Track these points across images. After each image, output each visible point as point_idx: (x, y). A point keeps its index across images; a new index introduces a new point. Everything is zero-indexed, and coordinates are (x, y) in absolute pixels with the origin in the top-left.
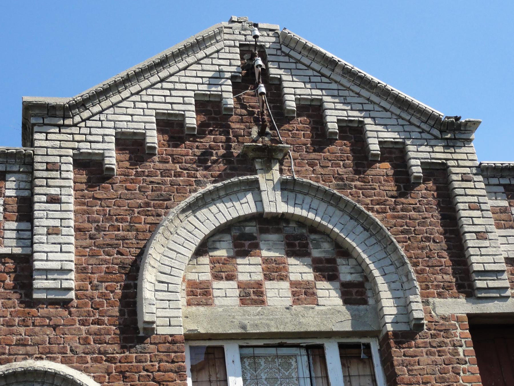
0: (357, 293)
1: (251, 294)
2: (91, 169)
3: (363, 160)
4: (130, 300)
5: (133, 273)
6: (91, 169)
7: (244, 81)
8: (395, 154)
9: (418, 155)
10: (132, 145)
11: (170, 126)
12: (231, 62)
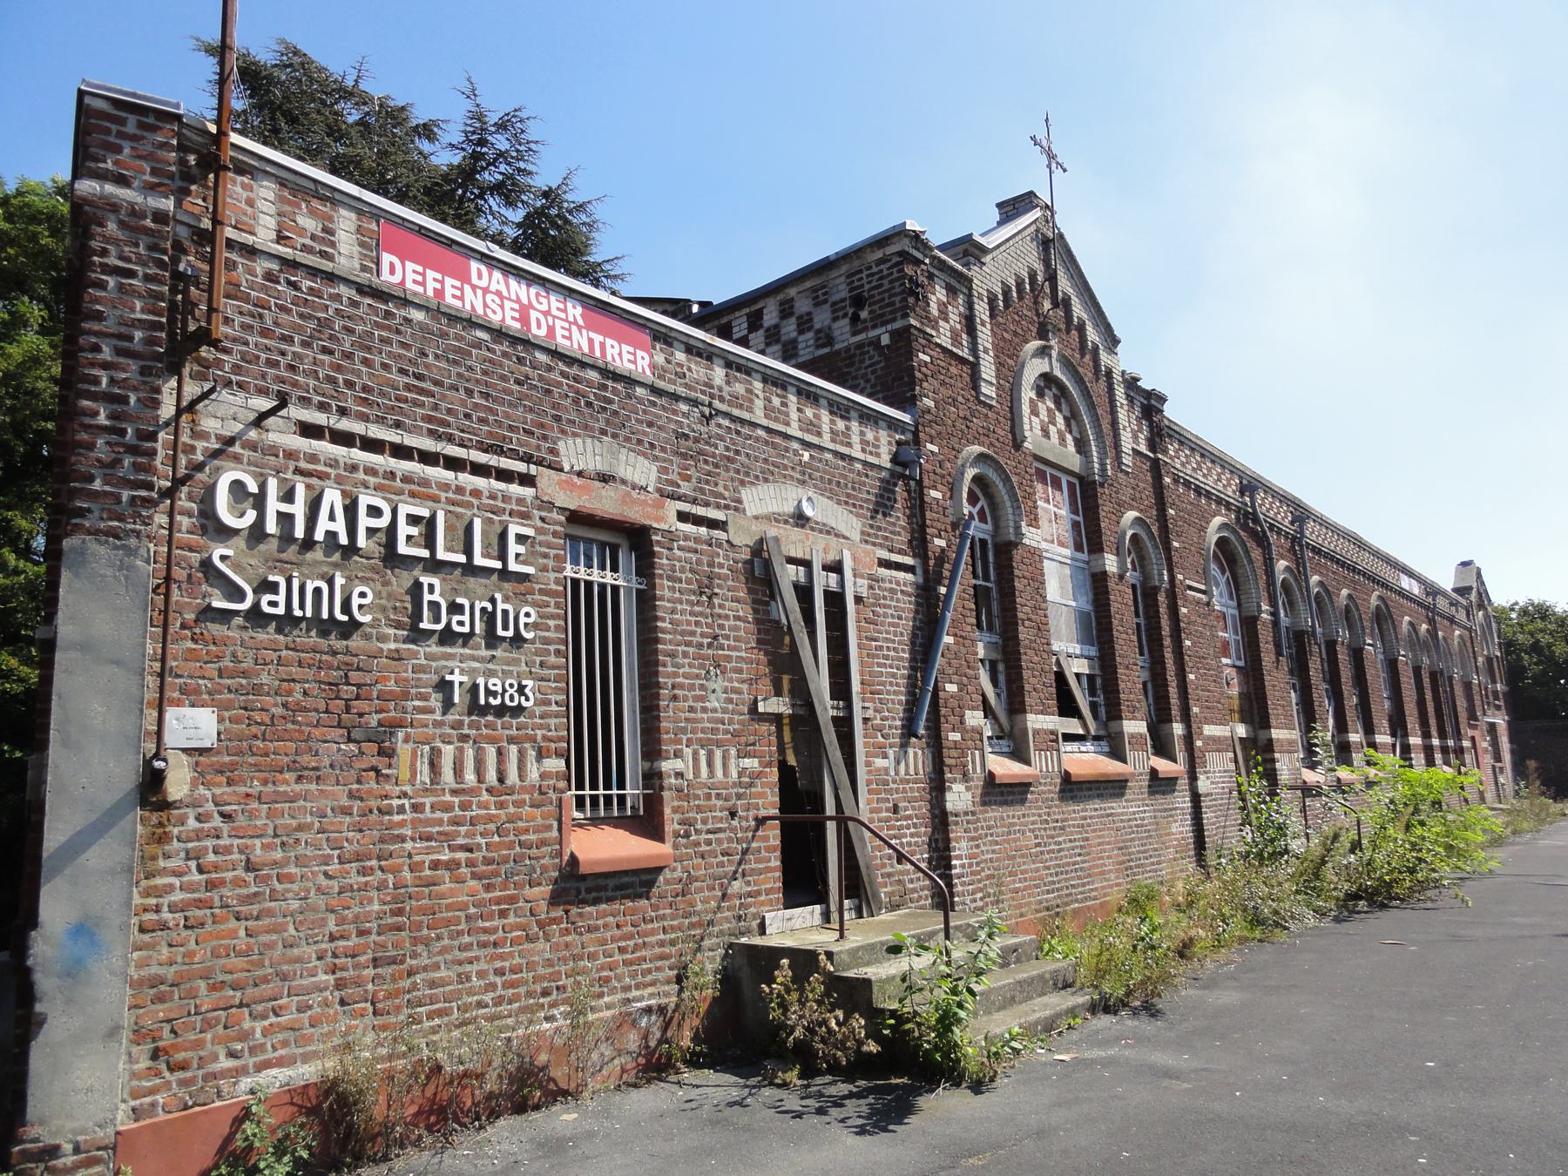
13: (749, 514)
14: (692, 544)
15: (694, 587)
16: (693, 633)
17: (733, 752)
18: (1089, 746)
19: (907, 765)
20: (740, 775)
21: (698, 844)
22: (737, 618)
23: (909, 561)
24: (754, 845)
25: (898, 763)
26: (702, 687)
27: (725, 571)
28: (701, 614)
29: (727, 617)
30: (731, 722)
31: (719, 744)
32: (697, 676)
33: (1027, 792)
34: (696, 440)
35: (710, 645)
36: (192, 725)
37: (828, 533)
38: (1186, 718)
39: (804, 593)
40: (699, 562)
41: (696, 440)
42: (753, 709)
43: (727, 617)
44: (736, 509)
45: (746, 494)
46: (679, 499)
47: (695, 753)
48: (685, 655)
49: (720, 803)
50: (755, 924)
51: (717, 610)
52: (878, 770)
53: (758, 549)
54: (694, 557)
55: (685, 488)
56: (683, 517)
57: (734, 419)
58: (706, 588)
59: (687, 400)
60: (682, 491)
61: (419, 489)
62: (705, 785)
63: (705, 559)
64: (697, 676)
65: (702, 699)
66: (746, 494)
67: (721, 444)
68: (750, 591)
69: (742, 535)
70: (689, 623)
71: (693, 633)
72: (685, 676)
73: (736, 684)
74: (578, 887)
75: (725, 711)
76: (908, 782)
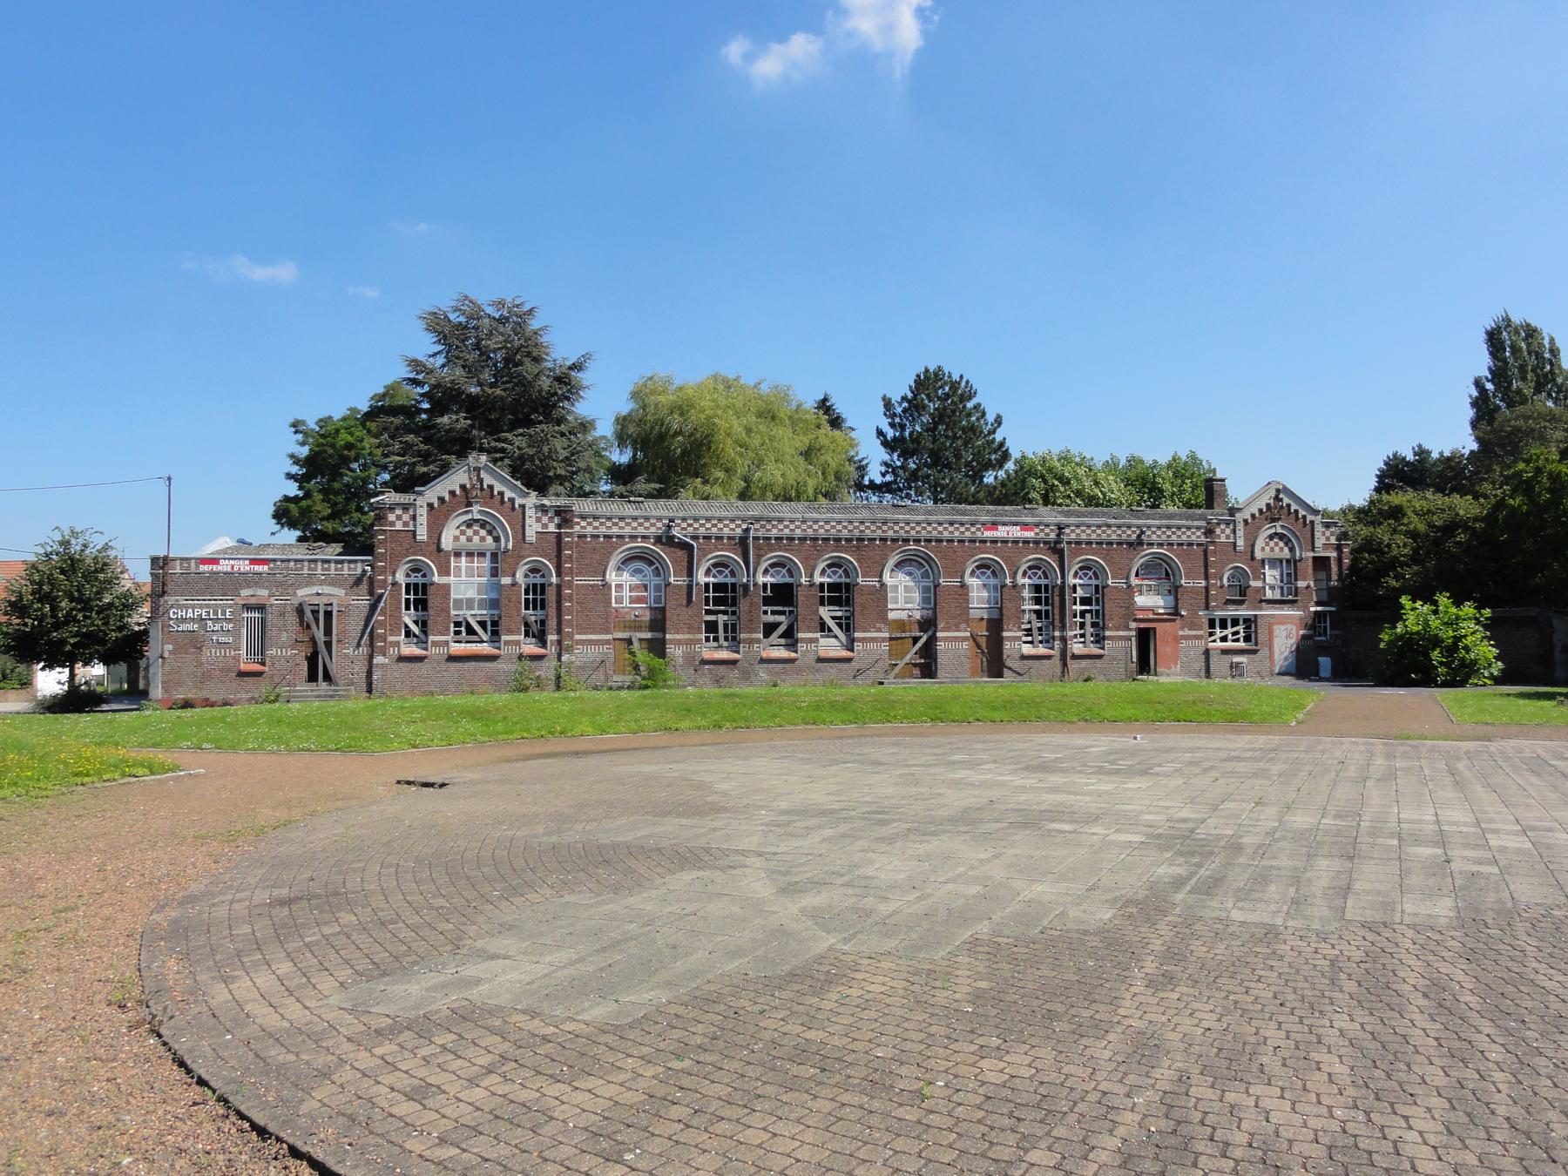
0: (1292, 550)
1: (1272, 549)
2: (1246, 521)
3: (1297, 519)
4: (1253, 552)
5: (1253, 546)
6: (1246, 521)
7: (1277, 499)
8: (1304, 517)
9: (1310, 518)
10: (1253, 516)
11: (1261, 511)
12: (1273, 493)
36: (170, 647)
38: (559, 632)
39: (315, 613)
58: (283, 614)
61: (208, 606)
69: (296, 602)
74: (242, 674)
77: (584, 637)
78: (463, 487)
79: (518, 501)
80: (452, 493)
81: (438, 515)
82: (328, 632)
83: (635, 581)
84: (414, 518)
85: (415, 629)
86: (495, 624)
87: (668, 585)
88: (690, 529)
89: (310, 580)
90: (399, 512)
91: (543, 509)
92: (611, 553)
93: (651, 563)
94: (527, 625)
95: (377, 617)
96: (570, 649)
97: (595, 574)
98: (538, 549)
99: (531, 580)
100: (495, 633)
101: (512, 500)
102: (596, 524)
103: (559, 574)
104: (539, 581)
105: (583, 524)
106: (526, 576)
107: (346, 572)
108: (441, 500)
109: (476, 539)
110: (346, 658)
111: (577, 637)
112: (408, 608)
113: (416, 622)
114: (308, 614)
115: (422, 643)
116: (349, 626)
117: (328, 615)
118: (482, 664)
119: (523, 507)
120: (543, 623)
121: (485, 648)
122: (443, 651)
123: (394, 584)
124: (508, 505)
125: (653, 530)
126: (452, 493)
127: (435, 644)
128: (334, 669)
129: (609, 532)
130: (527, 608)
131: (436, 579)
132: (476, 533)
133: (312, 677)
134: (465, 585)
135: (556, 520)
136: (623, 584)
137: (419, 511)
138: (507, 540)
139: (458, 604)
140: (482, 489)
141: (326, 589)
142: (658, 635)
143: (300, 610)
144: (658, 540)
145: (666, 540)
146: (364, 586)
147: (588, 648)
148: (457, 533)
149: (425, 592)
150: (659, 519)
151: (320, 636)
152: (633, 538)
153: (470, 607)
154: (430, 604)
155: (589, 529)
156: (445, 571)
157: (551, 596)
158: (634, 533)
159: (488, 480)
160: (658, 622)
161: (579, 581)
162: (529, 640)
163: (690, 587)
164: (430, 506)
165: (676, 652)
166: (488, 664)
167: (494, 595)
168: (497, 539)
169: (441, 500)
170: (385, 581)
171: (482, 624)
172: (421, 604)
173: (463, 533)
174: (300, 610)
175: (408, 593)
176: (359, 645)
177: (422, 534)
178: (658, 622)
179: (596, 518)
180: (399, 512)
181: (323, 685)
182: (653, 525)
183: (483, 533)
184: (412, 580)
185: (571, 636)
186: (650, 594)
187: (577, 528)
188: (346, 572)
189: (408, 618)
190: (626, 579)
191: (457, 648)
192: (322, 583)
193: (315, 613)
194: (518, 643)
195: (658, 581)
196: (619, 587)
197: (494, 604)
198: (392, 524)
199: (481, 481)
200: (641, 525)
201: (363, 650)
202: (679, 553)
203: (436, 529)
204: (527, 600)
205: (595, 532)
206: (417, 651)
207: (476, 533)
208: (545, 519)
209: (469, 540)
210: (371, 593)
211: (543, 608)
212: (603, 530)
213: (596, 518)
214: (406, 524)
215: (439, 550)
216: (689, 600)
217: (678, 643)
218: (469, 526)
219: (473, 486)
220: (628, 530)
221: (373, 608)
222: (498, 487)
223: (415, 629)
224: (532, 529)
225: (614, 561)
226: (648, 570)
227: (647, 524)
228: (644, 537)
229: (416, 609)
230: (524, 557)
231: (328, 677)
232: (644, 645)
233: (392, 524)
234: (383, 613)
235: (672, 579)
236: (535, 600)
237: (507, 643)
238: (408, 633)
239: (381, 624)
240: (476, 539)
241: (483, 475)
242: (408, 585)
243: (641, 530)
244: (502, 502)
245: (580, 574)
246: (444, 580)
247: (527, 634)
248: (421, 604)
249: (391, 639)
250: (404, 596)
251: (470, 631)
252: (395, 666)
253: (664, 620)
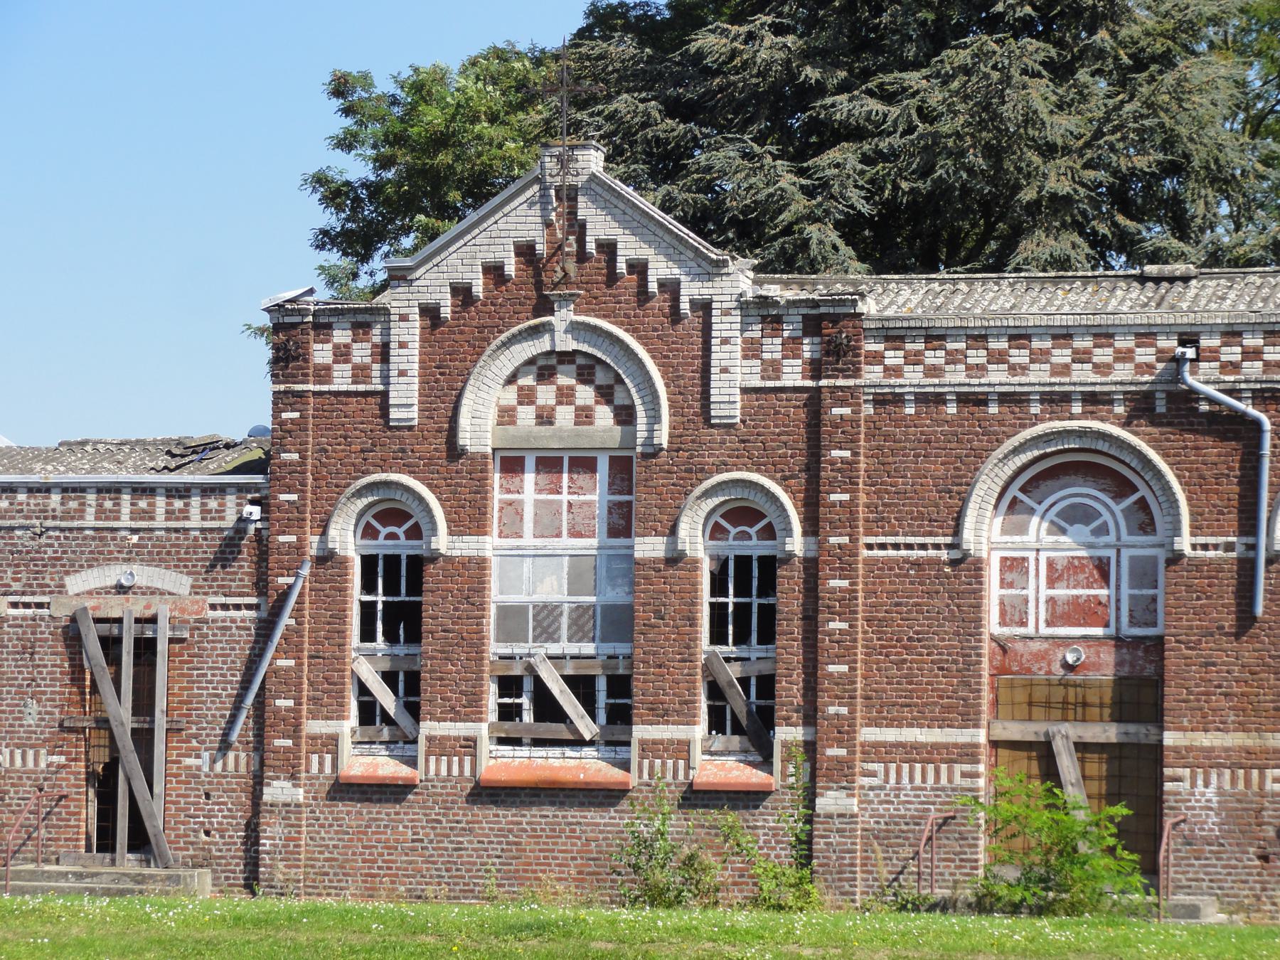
13: (70, 593)
14: (19, 622)
15: (20, 649)
16: (16, 679)
17: (43, 751)
18: (589, 751)
19: (225, 765)
20: (48, 766)
21: (10, 805)
22: (53, 666)
23: (254, 600)
24: (56, 810)
25: (213, 761)
26: (20, 712)
27: (46, 636)
28: (23, 666)
29: (45, 666)
30: (42, 733)
31: (32, 747)
32: (17, 705)
33: (406, 794)
34: (28, 552)
35: (28, 685)
37: (153, 593)
38: (810, 716)
39: (111, 645)
40: (24, 633)
41: (28, 552)
42: (61, 725)
43: (45, 666)
44: (60, 592)
45: (69, 581)
46: (11, 594)
47: (12, 753)
48: (9, 693)
49: (30, 782)
50: (53, 857)
51: (37, 662)
52: (189, 767)
53: (73, 619)
54: (20, 630)
55: (16, 586)
56: (15, 605)
57: (62, 530)
58: (28, 649)
59: (21, 527)
60: (14, 589)
62: (18, 771)
63: (29, 631)
64: (17, 705)
65: (20, 719)
66: (69, 581)
67: (50, 550)
68: (67, 646)
69: (62, 610)
70: (13, 672)
71: (16, 679)
72: (8, 705)
73: (49, 709)
75: (38, 726)
76: (225, 777)
77: (890, 735)
78: (525, 251)
79: (691, 290)
80: (494, 271)
81: (456, 339)
82: (144, 703)
83: (1070, 546)
84: (383, 354)
85: (387, 699)
86: (620, 685)
87: (1175, 558)
88: (1253, 369)
89: (102, 547)
90: (341, 336)
91: (763, 313)
92: (981, 456)
93: (1122, 487)
94: (715, 691)
95: (276, 660)
96: (843, 774)
97: (929, 523)
98: (748, 443)
99: (732, 547)
100: (621, 716)
101: (671, 288)
102: (934, 358)
103: (812, 526)
104: (756, 547)
105: (894, 358)
106: (717, 532)
107: (195, 521)
108: (462, 293)
109: (565, 415)
110: (190, 779)
111: (868, 734)
112: (367, 634)
113: (389, 678)
114: (93, 647)
115: (403, 743)
116: (198, 689)
117: (146, 649)
118: (573, 814)
119: (704, 307)
120: (767, 685)
121: (588, 765)
122: (459, 767)
123: (326, 558)
124: (660, 303)
125: (1123, 372)
126: (494, 271)
127: (439, 746)
128: (155, 814)
129: (977, 384)
130: (718, 637)
131: (442, 541)
132: (565, 396)
133: (106, 842)
134: (530, 563)
135: (808, 349)
136: (1026, 567)
137: (399, 332)
138: (655, 418)
139: (512, 618)
140: (582, 256)
141: (143, 575)
142: (1138, 732)
143: (72, 636)
144: (1141, 407)
145: (1167, 406)
146: (244, 566)
147: (907, 771)
148: (510, 396)
149: (416, 586)
150: (1146, 335)
151: (122, 714)
152: (1056, 400)
153: (547, 633)
154: (427, 624)
155: (913, 377)
156: (470, 518)
157: (789, 599)
158: (1061, 383)
159: (599, 226)
160: (1140, 693)
161: (872, 548)
162: (719, 742)
163: (1246, 568)
164: (430, 313)
165: (1194, 796)
166: (593, 816)
167: (616, 595)
168: (625, 416)
169: (462, 293)
170: (299, 548)
171: (581, 686)
172: (403, 621)
173: (527, 397)
174: (72, 636)
175: (368, 587)
176: (225, 746)
177: (406, 401)
178: (1140, 693)
179: (934, 337)
180: (341, 336)
181: (129, 862)
182: (1124, 356)
183: (585, 394)
184: (381, 546)
185: (845, 733)
186: (1118, 594)
187: (872, 374)
188: (195, 521)
189: (366, 664)
190: (1040, 538)
191: (502, 763)
192: (132, 555)
193: (111, 645)
194: (682, 749)
195: (1140, 547)
196: (1014, 566)
197: (617, 623)
198: (324, 374)
199: (580, 229)
200: (1082, 357)
201: (239, 760)
202: (1213, 449)
203: (444, 390)
204: (718, 612)
205: (931, 385)
206: (385, 766)
207: (565, 396)
208: (772, 349)
209: (545, 418)
210: (261, 585)
211: (767, 636)
212: (956, 376)
213: (934, 337)
214: (360, 373)
215: (454, 451)
216: (1246, 618)
217: (1207, 761)
218: (546, 374)
219: (557, 248)
220: (1039, 375)
221: (265, 628)
222: (630, 248)
223: (387, 699)
224: (733, 376)
225: (989, 482)
226: (1113, 511)
227: (1103, 355)
228: (1094, 400)
229: (391, 637)
230: (705, 472)
231: (140, 841)
232: (1097, 767)
233: (324, 374)
234: (291, 646)
235: (1184, 543)
236: (742, 612)
237: (649, 748)
238: (369, 711)
239: (290, 683)
240: (565, 415)
241: (585, 210)
242: (369, 563)
243: (1083, 375)
244: (643, 295)
245: (878, 523)
246: (464, 547)
247: (717, 723)
248: (403, 621)
249: (314, 727)
250: (356, 594)
251: (547, 708)
252: (326, 813)
253: (1158, 683)
